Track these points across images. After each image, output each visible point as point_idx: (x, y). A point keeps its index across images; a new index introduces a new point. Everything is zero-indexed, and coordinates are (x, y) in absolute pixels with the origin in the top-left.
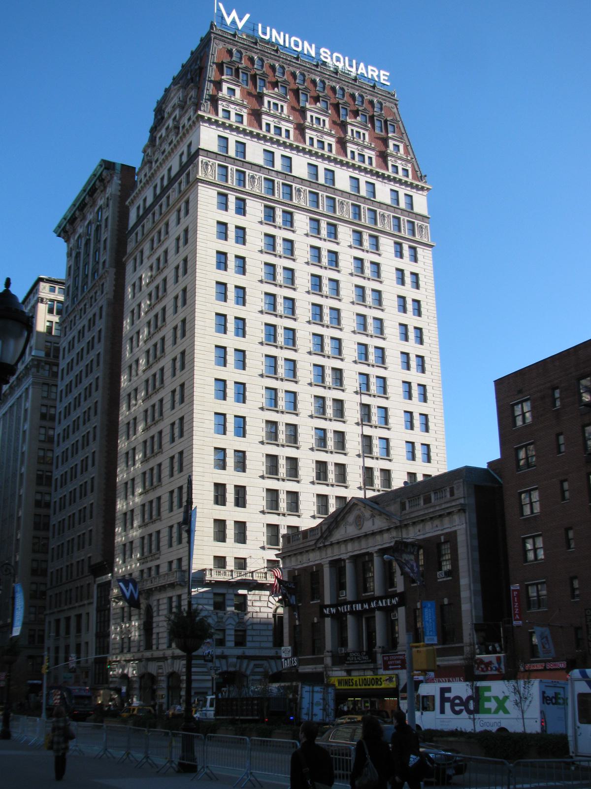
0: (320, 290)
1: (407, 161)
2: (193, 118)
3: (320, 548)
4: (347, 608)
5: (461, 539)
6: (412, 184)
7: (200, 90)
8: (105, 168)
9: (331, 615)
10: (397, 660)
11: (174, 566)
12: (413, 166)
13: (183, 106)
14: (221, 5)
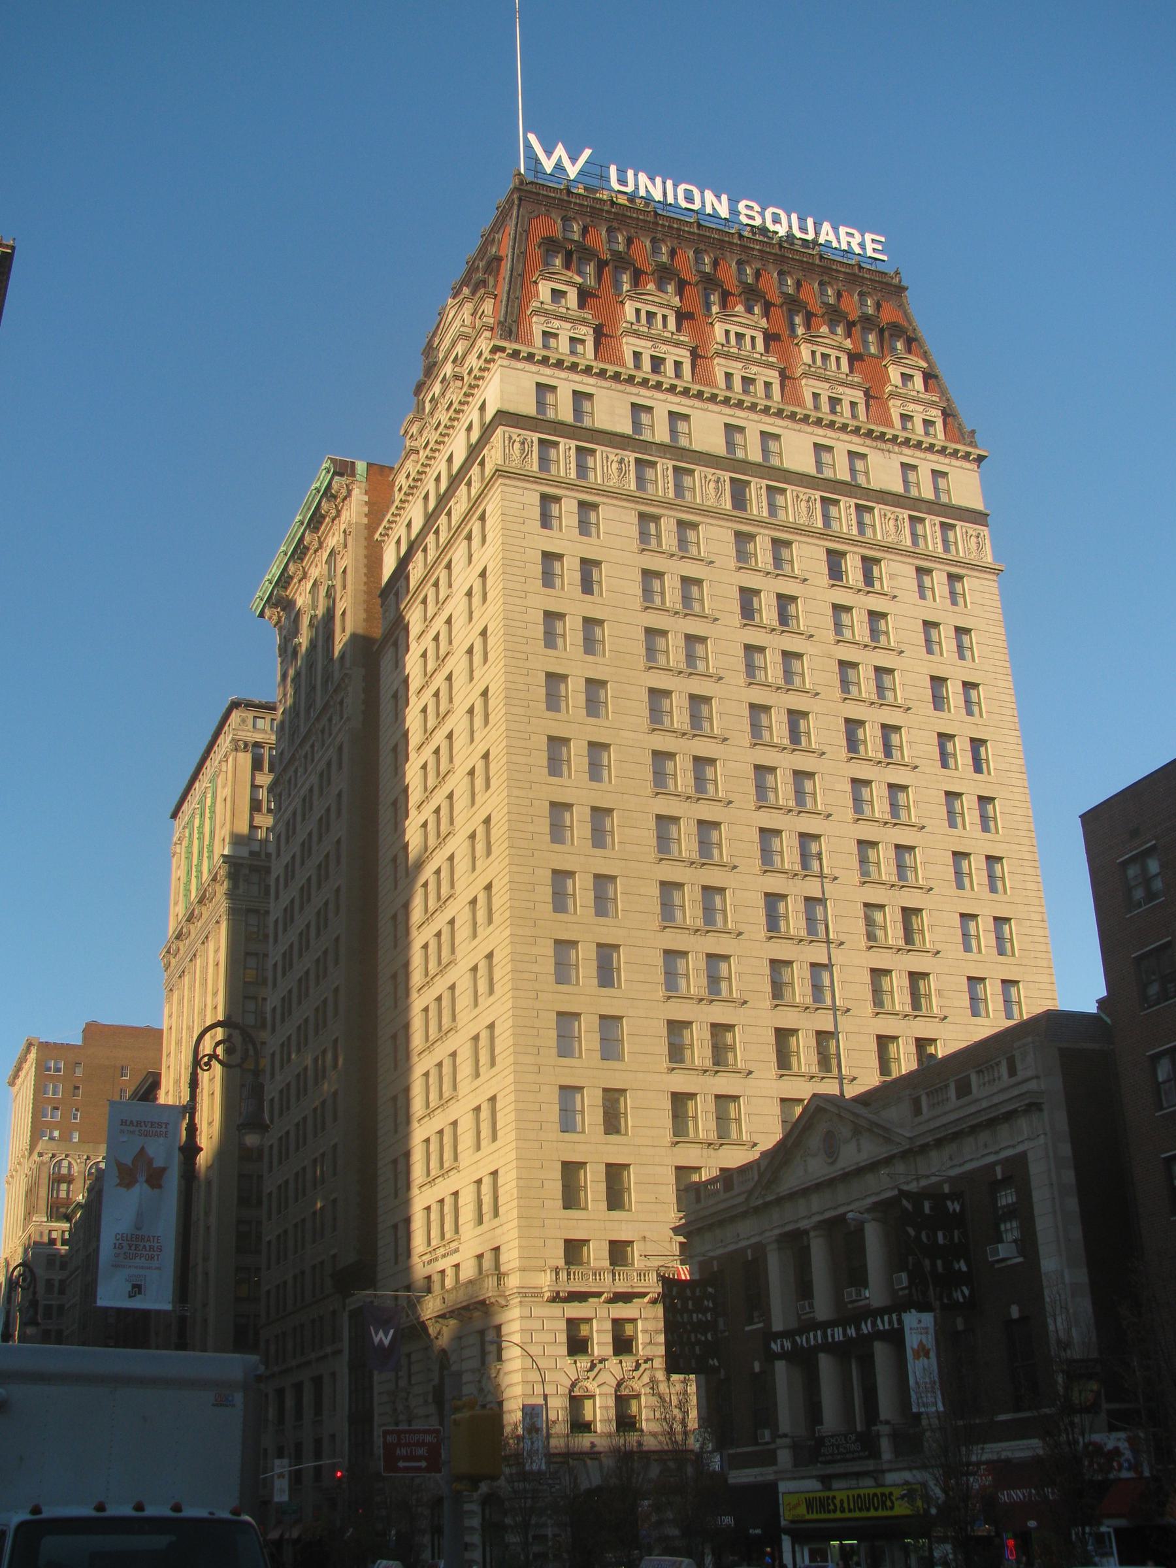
1: (932, 404)
4: (815, 1337)
5: (1038, 1171)
8: (335, 473)
9: (783, 1355)
10: (420, 1444)
14: (532, 138)
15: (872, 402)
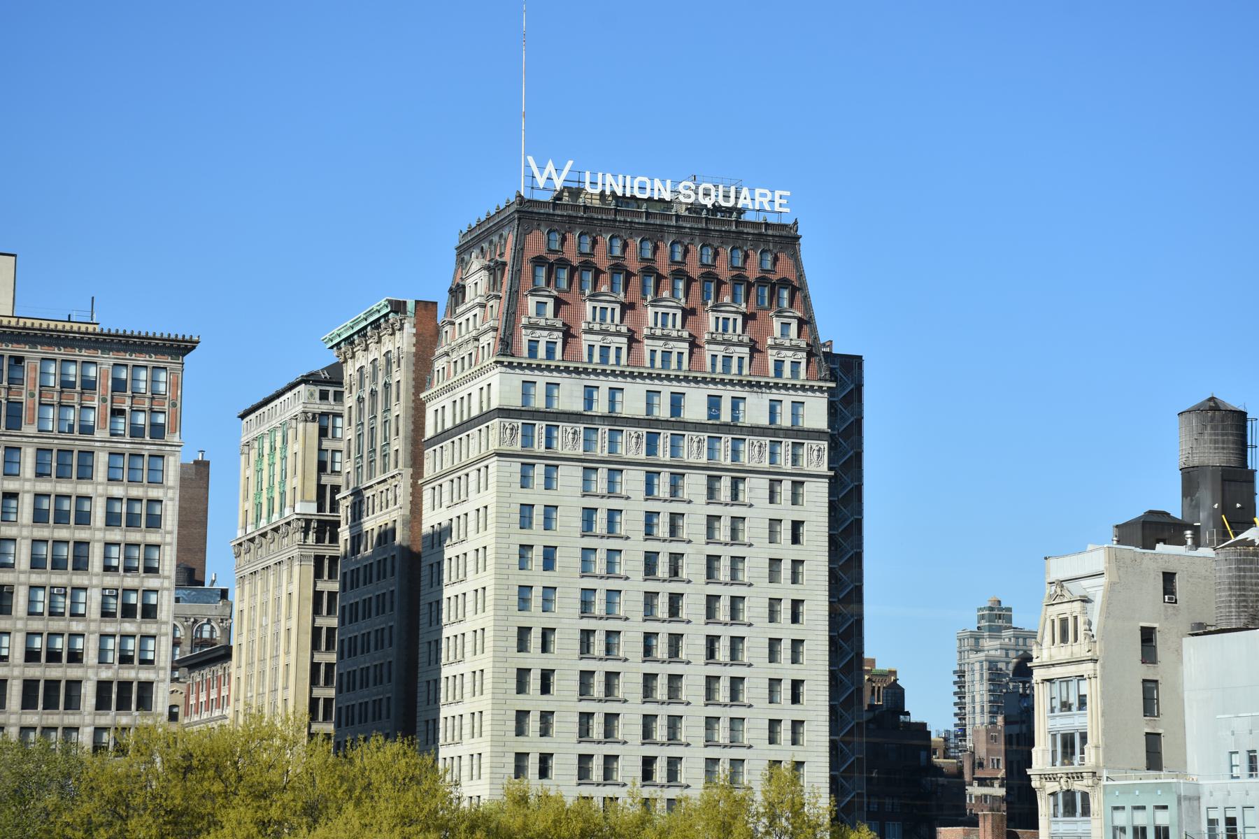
14: (530, 158)
15: (756, 355)
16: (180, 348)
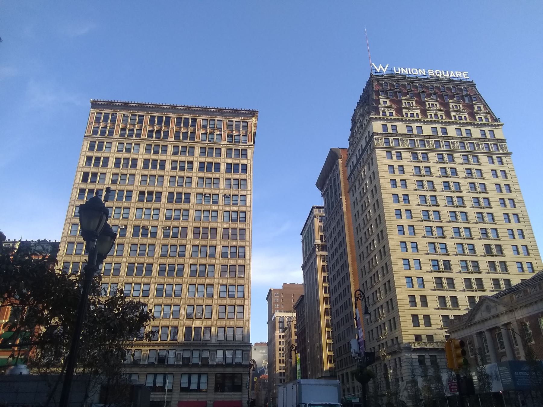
0: (450, 189)
1: (487, 113)
2: (368, 119)
3: (469, 326)
6: (492, 124)
7: (369, 105)
11: (395, 342)
12: (491, 115)
13: (363, 115)
16: (252, 113)
